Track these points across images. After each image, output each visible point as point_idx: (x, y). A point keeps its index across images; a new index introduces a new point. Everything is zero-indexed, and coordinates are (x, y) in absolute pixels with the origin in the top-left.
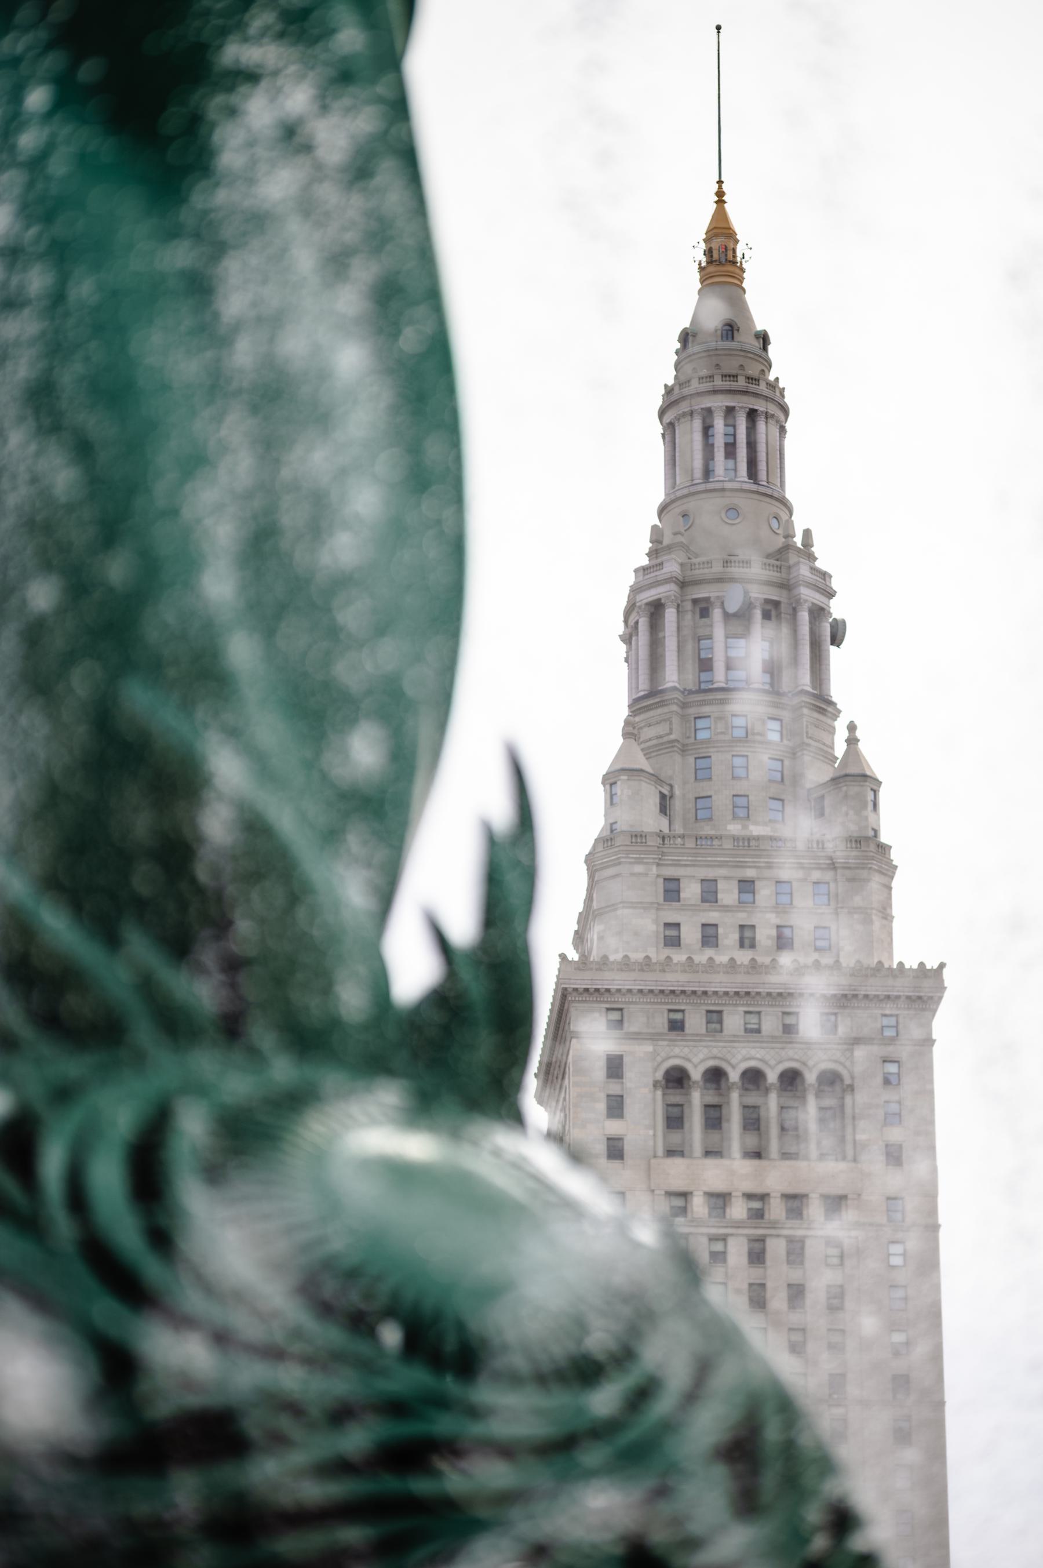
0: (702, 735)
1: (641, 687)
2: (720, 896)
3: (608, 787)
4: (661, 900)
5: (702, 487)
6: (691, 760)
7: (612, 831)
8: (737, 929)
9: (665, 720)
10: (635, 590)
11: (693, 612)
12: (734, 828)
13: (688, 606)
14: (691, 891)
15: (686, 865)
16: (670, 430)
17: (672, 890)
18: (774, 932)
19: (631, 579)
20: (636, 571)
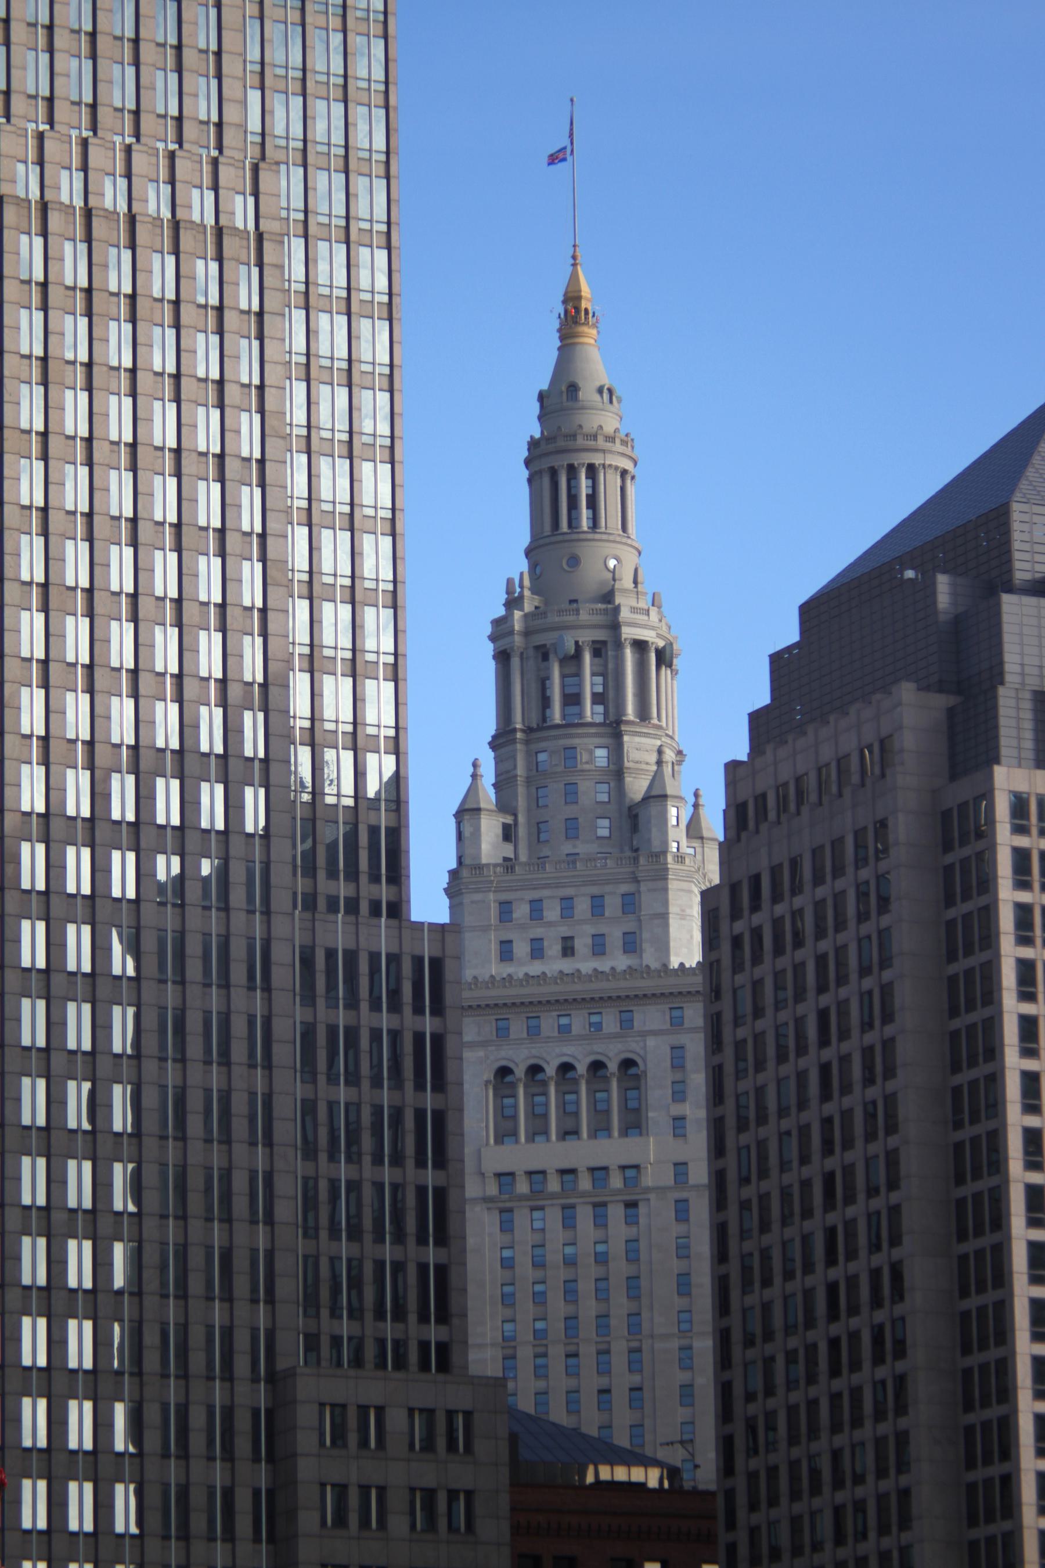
2: (545, 914)
12: (567, 848)
13: (531, 652)
17: (505, 910)
18: (589, 941)
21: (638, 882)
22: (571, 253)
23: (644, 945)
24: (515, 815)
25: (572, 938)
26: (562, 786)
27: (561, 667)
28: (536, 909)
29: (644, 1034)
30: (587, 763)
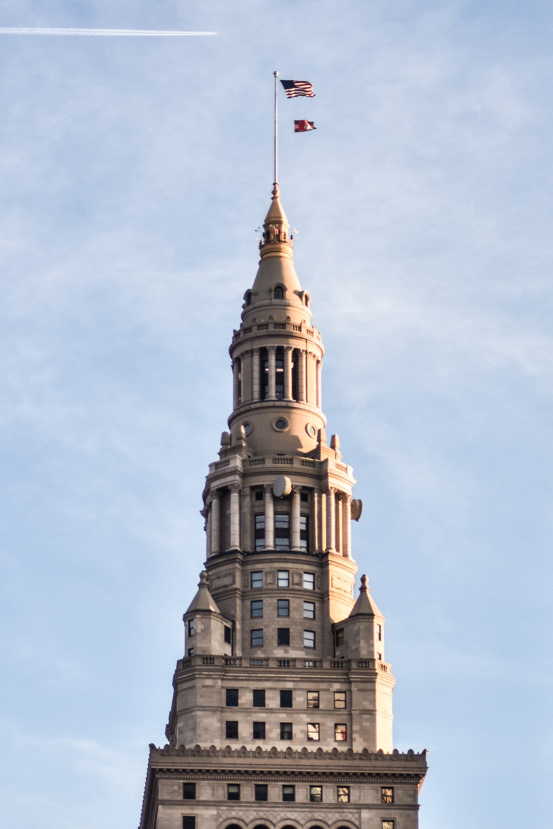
0: (257, 585)
1: (213, 550)
2: (267, 702)
3: (187, 623)
4: (224, 705)
5: (259, 405)
6: (248, 603)
7: (190, 654)
8: (279, 726)
9: (230, 574)
10: (210, 479)
11: (251, 496)
12: (279, 653)
13: (247, 491)
14: (246, 698)
15: (242, 680)
16: (237, 363)
19: (207, 472)
20: (210, 466)
21: (350, 683)
22: (272, 190)
23: (354, 736)
24: (234, 623)
25: (290, 724)
26: (275, 601)
27: (275, 505)
28: (259, 698)
29: (360, 807)
30: (297, 584)
